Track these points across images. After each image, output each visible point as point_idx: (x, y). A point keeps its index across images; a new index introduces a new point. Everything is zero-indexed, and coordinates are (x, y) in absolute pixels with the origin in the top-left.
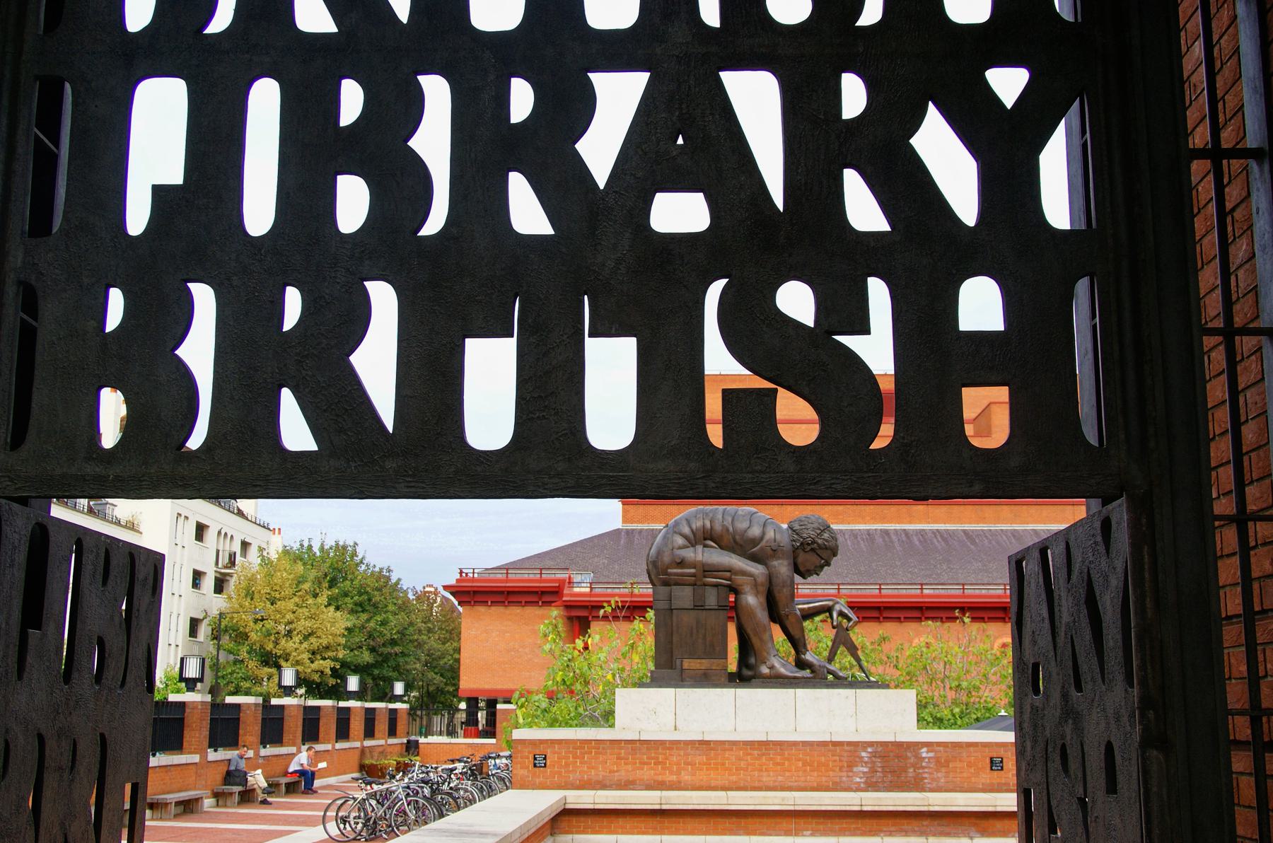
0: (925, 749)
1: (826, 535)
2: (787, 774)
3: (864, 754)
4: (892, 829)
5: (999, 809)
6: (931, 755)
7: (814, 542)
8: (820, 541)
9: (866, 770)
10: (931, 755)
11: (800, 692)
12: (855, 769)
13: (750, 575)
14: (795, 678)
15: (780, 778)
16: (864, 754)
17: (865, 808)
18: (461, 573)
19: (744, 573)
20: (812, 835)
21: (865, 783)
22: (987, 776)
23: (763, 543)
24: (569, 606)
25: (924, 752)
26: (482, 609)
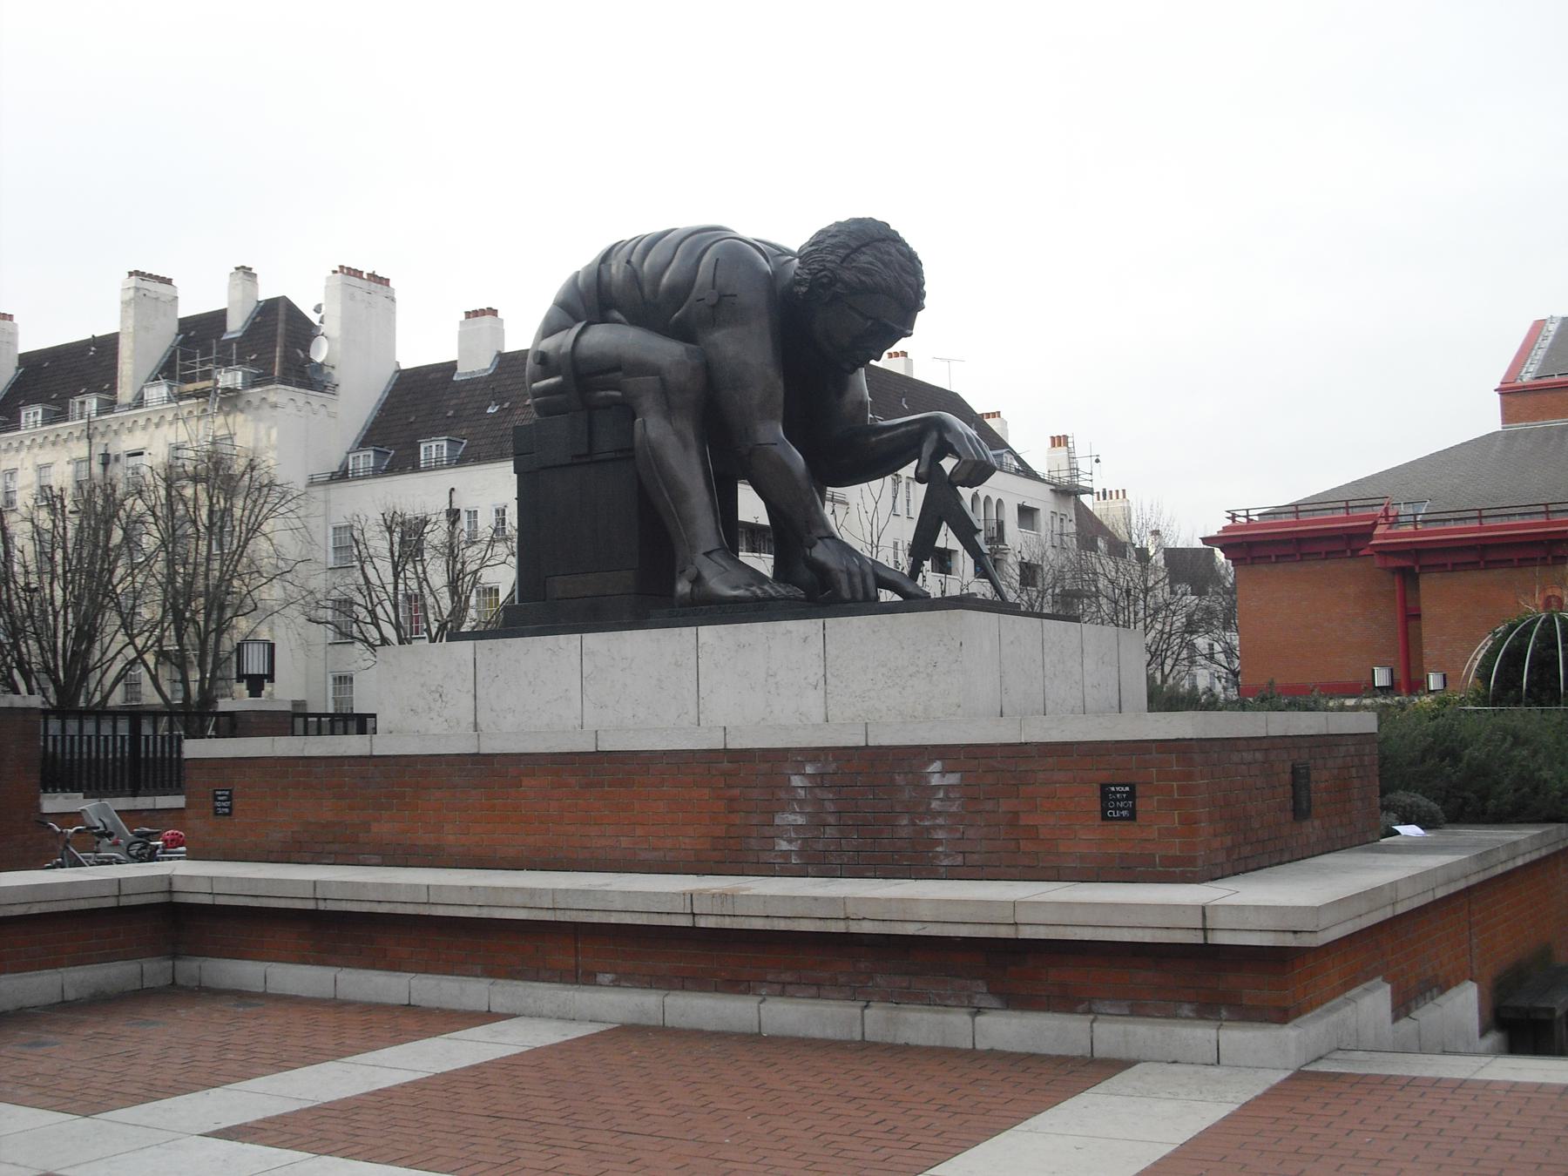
0: (936, 766)
1: (864, 259)
2: (639, 831)
3: (796, 781)
4: (787, 977)
5: (1026, 933)
6: (953, 779)
7: (834, 280)
8: (846, 275)
9: (800, 820)
10: (953, 779)
11: (707, 632)
12: (779, 819)
13: (656, 371)
14: (736, 600)
15: (625, 842)
16: (796, 781)
17: (703, 923)
18: (1233, 518)
19: (640, 368)
20: (615, 984)
21: (800, 853)
22: (1089, 837)
23: (694, 294)
24: (1385, 551)
25: (935, 774)
26: (1264, 568)
